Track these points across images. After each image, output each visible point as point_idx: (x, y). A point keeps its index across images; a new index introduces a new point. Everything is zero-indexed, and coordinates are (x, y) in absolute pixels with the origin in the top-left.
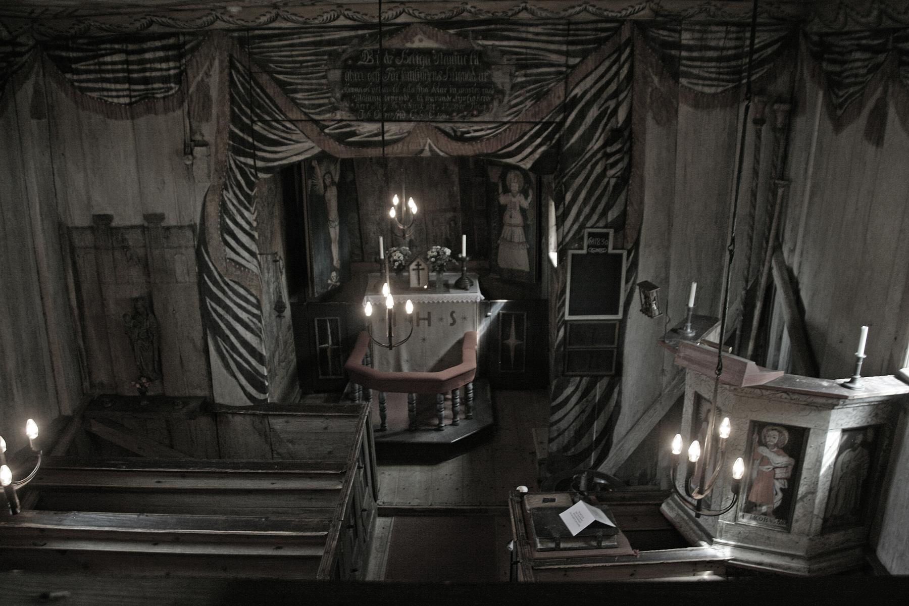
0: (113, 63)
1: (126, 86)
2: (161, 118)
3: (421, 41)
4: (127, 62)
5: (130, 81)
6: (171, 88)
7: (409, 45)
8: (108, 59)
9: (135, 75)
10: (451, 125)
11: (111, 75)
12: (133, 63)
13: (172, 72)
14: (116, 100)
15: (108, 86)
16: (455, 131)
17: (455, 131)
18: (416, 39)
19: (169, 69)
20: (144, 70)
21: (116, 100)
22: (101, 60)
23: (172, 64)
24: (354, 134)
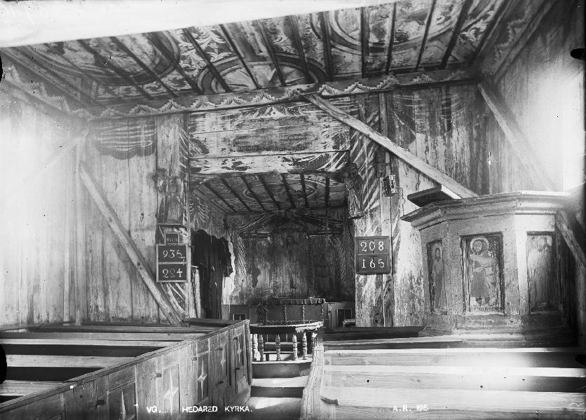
0: (121, 131)
1: (127, 143)
2: (144, 157)
3: (274, 113)
4: (128, 131)
5: (129, 140)
6: (149, 143)
7: (268, 116)
8: (119, 129)
9: (132, 137)
10: (291, 156)
11: (119, 137)
12: (131, 131)
13: (150, 135)
14: (120, 150)
15: (118, 142)
16: (293, 159)
17: (293, 159)
18: (272, 113)
19: (149, 133)
20: (136, 134)
21: (120, 150)
22: (116, 130)
23: (150, 131)
24: (240, 163)
